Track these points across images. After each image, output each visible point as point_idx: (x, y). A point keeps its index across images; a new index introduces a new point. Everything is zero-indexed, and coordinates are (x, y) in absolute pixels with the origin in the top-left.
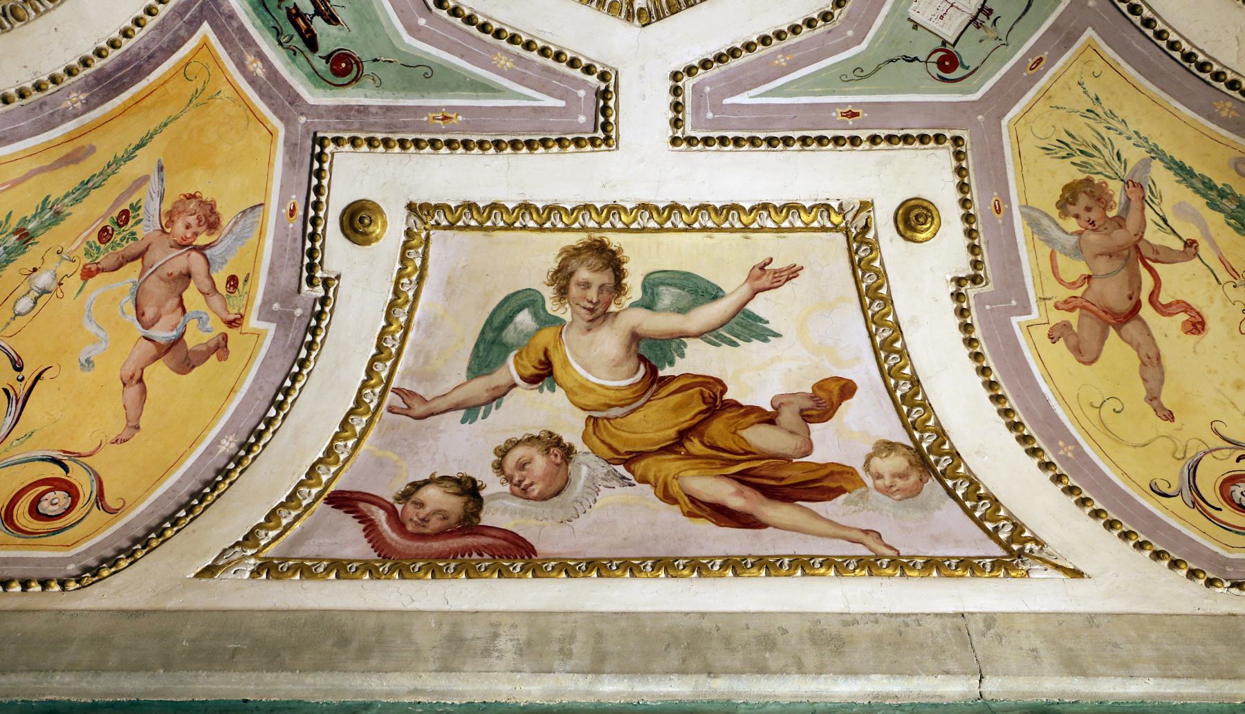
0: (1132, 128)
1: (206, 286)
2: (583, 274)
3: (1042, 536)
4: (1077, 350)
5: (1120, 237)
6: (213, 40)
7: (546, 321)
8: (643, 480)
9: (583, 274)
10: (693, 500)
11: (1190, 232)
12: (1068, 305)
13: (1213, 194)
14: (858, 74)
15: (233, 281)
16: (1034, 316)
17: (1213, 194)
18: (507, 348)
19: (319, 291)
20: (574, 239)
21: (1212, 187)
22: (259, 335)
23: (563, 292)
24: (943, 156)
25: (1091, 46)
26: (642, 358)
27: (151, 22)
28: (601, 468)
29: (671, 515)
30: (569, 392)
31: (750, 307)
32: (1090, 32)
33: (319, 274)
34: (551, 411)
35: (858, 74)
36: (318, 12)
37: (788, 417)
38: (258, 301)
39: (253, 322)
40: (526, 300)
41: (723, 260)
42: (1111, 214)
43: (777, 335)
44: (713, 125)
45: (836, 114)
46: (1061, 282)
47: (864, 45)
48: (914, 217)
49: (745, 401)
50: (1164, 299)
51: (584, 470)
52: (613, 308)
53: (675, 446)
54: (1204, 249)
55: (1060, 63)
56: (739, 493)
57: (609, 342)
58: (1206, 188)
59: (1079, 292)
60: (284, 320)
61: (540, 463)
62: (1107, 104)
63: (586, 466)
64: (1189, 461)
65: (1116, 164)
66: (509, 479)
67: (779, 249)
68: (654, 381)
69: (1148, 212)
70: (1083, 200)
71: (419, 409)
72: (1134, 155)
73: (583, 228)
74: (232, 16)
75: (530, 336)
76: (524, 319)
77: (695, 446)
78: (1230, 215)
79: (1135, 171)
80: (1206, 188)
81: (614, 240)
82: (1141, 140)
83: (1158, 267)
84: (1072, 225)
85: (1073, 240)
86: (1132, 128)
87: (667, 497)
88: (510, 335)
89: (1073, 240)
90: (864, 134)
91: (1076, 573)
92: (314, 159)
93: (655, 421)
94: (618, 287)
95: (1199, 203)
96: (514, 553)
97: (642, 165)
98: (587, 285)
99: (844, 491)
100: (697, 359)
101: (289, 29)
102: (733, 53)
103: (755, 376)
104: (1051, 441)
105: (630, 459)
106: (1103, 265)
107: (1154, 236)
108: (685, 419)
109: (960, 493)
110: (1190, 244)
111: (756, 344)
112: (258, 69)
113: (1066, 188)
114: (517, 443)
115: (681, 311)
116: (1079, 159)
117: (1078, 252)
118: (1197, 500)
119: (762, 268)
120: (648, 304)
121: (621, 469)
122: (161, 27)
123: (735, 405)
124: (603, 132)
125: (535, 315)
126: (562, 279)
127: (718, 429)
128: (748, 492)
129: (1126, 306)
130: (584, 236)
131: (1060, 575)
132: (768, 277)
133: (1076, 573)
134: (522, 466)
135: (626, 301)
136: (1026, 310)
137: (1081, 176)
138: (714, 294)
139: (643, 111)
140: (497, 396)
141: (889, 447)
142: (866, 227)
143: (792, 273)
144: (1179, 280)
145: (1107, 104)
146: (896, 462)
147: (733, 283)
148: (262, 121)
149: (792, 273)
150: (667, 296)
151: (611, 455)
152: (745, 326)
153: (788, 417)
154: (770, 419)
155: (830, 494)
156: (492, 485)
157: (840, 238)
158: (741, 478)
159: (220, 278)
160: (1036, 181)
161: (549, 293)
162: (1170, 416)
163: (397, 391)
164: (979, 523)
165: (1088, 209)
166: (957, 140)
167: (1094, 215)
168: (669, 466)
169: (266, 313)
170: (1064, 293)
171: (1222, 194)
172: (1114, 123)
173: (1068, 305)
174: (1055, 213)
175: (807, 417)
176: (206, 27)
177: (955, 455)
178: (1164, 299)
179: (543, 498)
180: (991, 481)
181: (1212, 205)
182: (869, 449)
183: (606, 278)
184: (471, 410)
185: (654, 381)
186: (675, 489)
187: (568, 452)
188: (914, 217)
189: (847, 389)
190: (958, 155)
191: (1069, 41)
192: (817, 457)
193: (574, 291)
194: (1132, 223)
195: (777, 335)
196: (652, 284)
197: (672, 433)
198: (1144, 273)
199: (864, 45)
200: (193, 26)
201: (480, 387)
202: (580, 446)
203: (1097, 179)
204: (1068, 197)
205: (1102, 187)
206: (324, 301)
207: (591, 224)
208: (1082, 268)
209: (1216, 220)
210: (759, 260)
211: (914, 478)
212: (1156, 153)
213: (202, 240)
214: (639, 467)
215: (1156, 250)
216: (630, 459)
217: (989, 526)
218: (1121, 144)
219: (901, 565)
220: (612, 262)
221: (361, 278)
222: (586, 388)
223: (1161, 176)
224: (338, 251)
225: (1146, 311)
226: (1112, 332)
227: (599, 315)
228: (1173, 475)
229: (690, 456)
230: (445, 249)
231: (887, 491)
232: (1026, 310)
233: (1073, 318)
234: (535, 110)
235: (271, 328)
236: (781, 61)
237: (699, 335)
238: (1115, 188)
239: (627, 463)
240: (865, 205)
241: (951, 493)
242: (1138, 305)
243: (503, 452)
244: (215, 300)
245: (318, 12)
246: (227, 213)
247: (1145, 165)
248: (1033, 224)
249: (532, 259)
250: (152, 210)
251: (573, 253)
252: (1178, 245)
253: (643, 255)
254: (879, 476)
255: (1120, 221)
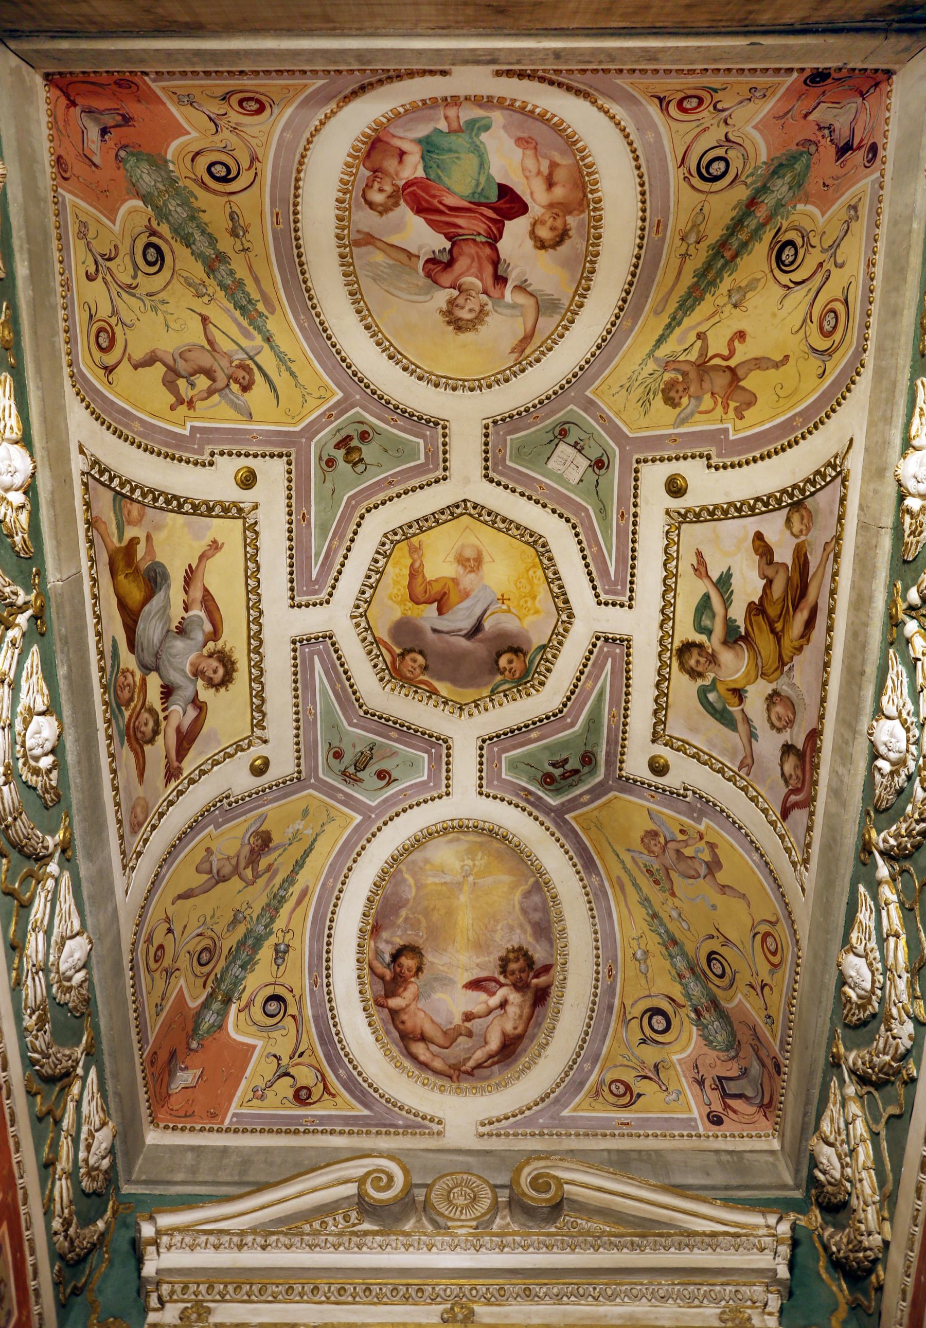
0: (637, 367)
1: (683, 844)
2: (692, 662)
3: (834, 453)
4: (749, 405)
5: (693, 375)
6: (573, 814)
7: (713, 687)
8: (792, 659)
9: (692, 662)
10: (802, 637)
11: (692, 337)
12: (726, 407)
13: (673, 324)
14: (603, 511)
15: (682, 832)
16: (730, 426)
17: (673, 324)
18: (725, 709)
19: (690, 793)
20: (675, 664)
21: (670, 324)
22: (708, 827)
23: (700, 675)
24: (645, 469)
25: (594, 392)
26: (735, 642)
27: (562, 840)
28: (784, 679)
29: (807, 650)
30: (749, 683)
31: (715, 579)
32: (588, 393)
33: (682, 792)
34: (757, 693)
35: (603, 511)
36: (563, 766)
37: (770, 572)
38: (692, 823)
39: (702, 828)
40: (703, 693)
41: (691, 590)
42: (681, 379)
43: (729, 569)
44: (624, 586)
45: (622, 523)
46: (713, 409)
47: (589, 507)
48: (675, 488)
49: (760, 593)
50: (726, 352)
51: (784, 687)
52: (710, 651)
53: (778, 637)
54: (702, 329)
55: (603, 406)
56: (802, 610)
57: (726, 656)
58: (670, 328)
59: (720, 400)
60: (702, 814)
61: (779, 709)
62: (624, 381)
63: (782, 685)
64: (810, 351)
65: (655, 376)
66: (785, 727)
67: (687, 561)
68: (746, 638)
69: (681, 358)
70: (672, 394)
71: (749, 761)
72: (651, 366)
73: (670, 658)
74: (563, 804)
75: (720, 696)
76: (711, 697)
77: (779, 626)
78: (685, 314)
79: (659, 366)
80: (670, 328)
81: (677, 644)
82: (644, 362)
83: (710, 354)
84: (685, 401)
85: (693, 400)
86: (637, 367)
87: (800, 649)
88: (718, 706)
89: (693, 400)
90: (632, 510)
91: (851, 440)
92: (629, 784)
93: (765, 642)
94: (700, 646)
95: (678, 331)
96: (815, 735)
97: (641, 624)
98: (698, 662)
99: (806, 555)
100: (738, 613)
101: (570, 780)
102: (589, 574)
103: (748, 585)
104: (794, 429)
105: (782, 663)
106: (707, 385)
107: (693, 356)
108: (765, 628)
109: (813, 489)
110: (699, 336)
111: (733, 581)
112: (586, 798)
113: (666, 403)
114: (769, 718)
115: (714, 616)
116: (651, 396)
117: (699, 398)
118: (827, 353)
119: (696, 570)
120: (709, 632)
121: (786, 668)
122: (566, 836)
123: (761, 599)
124: (625, 642)
125: (710, 691)
126: (694, 674)
127: (773, 612)
128: (801, 606)
129: (728, 373)
130: (674, 659)
131: (851, 451)
132: (701, 568)
133: (851, 440)
134: (780, 719)
135: (707, 644)
136: (726, 431)
137: (660, 395)
138: (706, 598)
139: (615, 621)
140: (747, 720)
141: (788, 521)
142: (679, 513)
143: (699, 554)
144: (718, 345)
145: (624, 381)
146: (796, 518)
147: (702, 587)
148: (610, 801)
149: (699, 554)
150: (706, 622)
151: (779, 672)
152: (724, 583)
153: (770, 572)
154: (770, 583)
155: (806, 563)
156: (786, 737)
157: (684, 526)
158: (796, 607)
159: (680, 837)
160: (661, 419)
161: (700, 682)
162: (787, 357)
163: (740, 769)
164: (828, 484)
165: (677, 391)
166: (638, 462)
167: (681, 388)
168: (786, 643)
169: (698, 820)
170: (719, 408)
171: (674, 319)
172: (634, 377)
173: (726, 407)
174: (678, 410)
175: (770, 562)
176: (567, 817)
177: (794, 487)
178: (726, 352)
179: (794, 713)
180: (807, 471)
181: (679, 324)
182: (788, 532)
183: (695, 652)
184: (752, 735)
185: (746, 638)
186: (796, 644)
187: (775, 693)
188: (675, 488)
189: (759, 536)
190: (645, 461)
191: (591, 402)
192: (790, 563)
193: (700, 669)
194: (686, 368)
195: (729, 569)
196: (700, 629)
197: (771, 636)
198: (713, 362)
199: (589, 507)
200: (566, 822)
201: (742, 727)
202: (773, 686)
203: (662, 386)
204: (671, 402)
205: (666, 384)
206: (694, 793)
207: (668, 654)
208: (707, 397)
209: (687, 322)
210: (692, 571)
211: (804, 512)
212: (651, 354)
213: (662, 840)
214: (786, 659)
215: (701, 355)
216: (782, 663)
217: (829, 479)
218: (645, 374)
219: (838, 538)
220: (687, 647)
221: (684, 772)
222: (747, 674)
223: (661, 353)
224: (670, 781)
225: (732, 363)
226: (741, 383)
227: (713, 659)
228: (815, 363)
229: (783, 630)
230: (675, 728)
231: (808, 529)
232: (726, 431)
233: (732, 405)
234: (612, 673)
235: (705, 820)
236: (595, 549)
237: (726, 610)
238: (667, 376)
239: (784, 665)
240: (667, 513)
241: (812, 494)
242: (728, 367)
243: (773, 726)
244: (690, 842)
245: (563, 766)
246: (651, 826)
247: (656, 360)
248: (683, 422)
249: (683, 688)
250: (646, 858)
251: (682, 666)
252: (699, 342)
253: (685, 631)
254: (801, 531)
255: (685, 374)
